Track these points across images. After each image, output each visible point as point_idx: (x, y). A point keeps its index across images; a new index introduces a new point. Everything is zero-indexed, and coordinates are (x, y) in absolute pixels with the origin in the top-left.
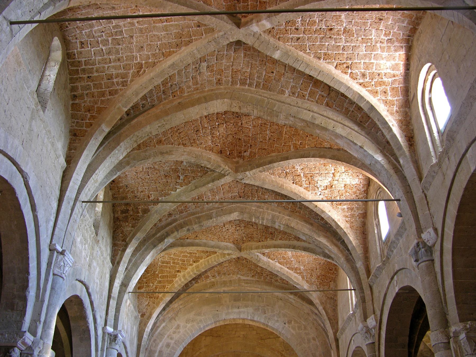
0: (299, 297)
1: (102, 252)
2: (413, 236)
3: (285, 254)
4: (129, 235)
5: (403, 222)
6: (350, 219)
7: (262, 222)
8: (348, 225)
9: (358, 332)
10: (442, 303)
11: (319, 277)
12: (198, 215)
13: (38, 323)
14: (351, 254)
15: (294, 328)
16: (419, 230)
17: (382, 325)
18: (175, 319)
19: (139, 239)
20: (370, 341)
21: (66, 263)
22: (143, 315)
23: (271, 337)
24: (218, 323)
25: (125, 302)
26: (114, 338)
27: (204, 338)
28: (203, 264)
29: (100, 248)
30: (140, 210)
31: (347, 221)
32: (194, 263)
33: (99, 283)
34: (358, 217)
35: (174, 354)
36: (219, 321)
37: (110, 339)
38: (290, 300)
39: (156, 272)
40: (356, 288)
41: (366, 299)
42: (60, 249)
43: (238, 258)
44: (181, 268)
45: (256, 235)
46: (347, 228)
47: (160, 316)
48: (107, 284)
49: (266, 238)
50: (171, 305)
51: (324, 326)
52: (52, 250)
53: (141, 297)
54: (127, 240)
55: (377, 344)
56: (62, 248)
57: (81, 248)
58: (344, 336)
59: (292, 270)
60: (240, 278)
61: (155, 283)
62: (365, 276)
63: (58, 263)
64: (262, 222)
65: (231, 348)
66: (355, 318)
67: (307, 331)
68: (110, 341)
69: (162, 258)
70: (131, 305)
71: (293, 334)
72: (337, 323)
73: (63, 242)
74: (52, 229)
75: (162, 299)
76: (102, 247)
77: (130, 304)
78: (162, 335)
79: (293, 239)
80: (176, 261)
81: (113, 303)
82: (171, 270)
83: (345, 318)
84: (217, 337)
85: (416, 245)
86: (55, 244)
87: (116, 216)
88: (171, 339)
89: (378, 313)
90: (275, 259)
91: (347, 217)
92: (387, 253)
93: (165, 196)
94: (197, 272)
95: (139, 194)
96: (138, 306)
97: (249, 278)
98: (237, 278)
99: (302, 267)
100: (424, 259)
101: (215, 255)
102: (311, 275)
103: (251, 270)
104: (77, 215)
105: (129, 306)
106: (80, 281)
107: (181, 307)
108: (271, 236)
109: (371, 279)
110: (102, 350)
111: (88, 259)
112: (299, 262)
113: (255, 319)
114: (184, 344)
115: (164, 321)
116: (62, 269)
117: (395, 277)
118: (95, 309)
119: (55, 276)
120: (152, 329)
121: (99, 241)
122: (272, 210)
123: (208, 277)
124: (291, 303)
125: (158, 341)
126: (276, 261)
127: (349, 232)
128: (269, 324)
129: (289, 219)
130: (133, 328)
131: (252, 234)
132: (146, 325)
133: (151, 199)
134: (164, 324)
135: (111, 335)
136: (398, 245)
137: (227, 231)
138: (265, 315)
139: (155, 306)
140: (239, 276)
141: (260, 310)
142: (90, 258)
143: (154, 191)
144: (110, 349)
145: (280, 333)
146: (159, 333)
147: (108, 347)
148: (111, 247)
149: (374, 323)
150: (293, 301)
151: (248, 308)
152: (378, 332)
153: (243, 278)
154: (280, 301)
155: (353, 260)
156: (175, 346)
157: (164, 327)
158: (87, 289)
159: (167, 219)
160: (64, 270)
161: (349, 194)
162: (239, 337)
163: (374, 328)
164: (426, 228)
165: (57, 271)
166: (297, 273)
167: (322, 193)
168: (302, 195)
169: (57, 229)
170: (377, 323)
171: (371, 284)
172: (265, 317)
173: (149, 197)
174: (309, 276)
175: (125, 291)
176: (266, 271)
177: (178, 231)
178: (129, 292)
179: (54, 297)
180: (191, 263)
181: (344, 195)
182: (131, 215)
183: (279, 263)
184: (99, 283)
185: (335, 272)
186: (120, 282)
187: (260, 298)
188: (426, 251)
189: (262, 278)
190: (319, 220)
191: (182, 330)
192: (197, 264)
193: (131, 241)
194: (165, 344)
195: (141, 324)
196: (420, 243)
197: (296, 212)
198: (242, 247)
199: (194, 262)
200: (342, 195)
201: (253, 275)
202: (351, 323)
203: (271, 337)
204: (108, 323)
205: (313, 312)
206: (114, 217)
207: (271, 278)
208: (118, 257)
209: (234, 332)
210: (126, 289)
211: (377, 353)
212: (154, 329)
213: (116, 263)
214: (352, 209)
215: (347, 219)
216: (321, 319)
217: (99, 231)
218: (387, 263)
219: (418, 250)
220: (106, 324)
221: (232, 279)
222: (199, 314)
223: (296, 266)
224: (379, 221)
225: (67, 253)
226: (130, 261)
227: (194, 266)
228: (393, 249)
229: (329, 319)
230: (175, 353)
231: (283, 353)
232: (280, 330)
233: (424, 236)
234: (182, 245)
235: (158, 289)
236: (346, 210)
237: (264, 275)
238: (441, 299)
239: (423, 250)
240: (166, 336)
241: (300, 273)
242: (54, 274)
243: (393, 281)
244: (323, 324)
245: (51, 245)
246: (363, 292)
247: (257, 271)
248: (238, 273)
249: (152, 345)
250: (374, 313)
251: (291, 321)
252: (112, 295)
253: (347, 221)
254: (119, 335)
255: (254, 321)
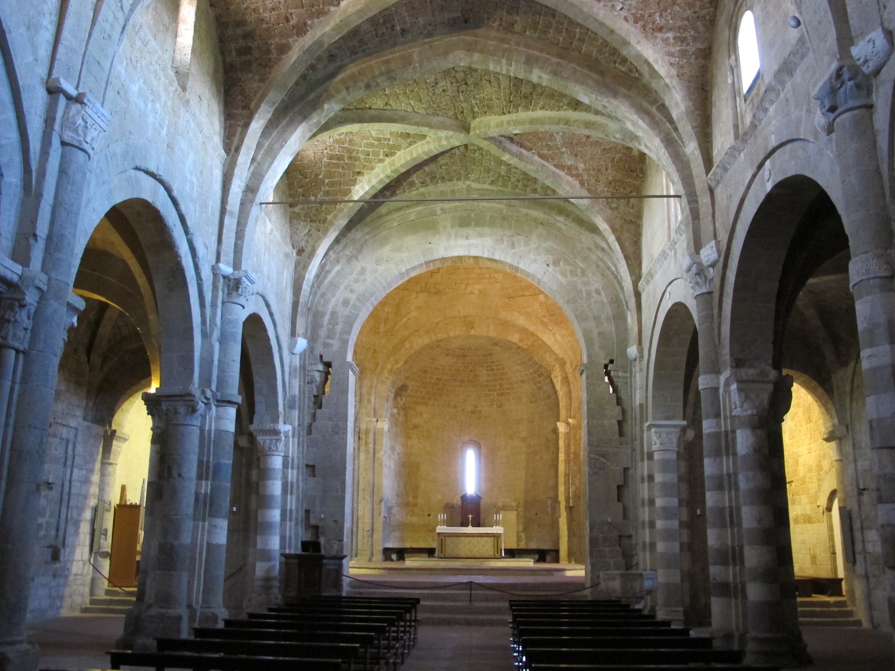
0: (574, 220)
1: (199, 125)
2: (826, 59)
3: (551, 140)
4: (255, 96)
5: (801, 41)
6: (677, 59)
7: (508, 71)
8: (674, 72)
9: (679, 276)
10: (883, 195)
11: (610, 183)
12: (385, 58)
13: (32, 241)
14: (676, 129)
15: (563, 273)
16: (845, 39)
17: (730, 260)
18: (357, 259)
19: (274, 103)
20: (704, 290)
21: (89, 121)
22: (300, 252)
23: (526, 293)
24: (431, 264)
25: (253, 221)
26: (234, 285)
27: (414, 296)
28: (403, 159)
29: (194, 116)
30: (273, 46)
31: (671, 64)
32: (386, 158)
33: (196, 183)
34: (694, 57)
35: (357, 316)
36: (434, 261)
37: (229, 286)
38: (558, 225)
39: (319, 175)
40: (682, 192)
41: (701, 213)
42: (73, 92)
43: (466, 146)
44: (364, 166)
45: (498, 101)
46: (671, 77)
47: (331, 253)
48: (217, 187)
49: (516, 107)
50: (349, 235)
51: (616, 269)
52: (54, 91)
53: (295, 221)
54: (252, 105)
55: (716, 295)
56: (77, 88)
57: (142, 106)
58: (651, 285)
59: (563, 170)
60: (469, 186)
61: (319, 196)
62: (702, 169)
63: (71, 120)
64: (508, 71)
65: (459, 312)
66: (675, 253)
67: (586, 279)
68: (228, 290)
69: (328, 148)
70: (275, 233)
71: (562, 283)
72: (640, 265)
73: (79, 78)
74: (50, 48)
75: (332, 224)
76: (197, 113)
77: (272, 230)
78: (334, 285)
79: (565, 107)
80: (354, 154)
81: (230, 223)
82: (347, 172)
83: (656, 255)
84: (435, 293)
85: (835, 74)
86: (57, 80)
87: (228, 60)
88: (352, 291)
89: (723, 237)
90: (532, 149)
91: (671, 55)
92: (754, 116)
93: (318, 18)
94: (392, 174)
95: (267, 15)
96: (291, 237)
97: (487, 186)
98: (464, 186)
99: (581, 166)
100: (851, 104)
101: (424, 141)
102: (597, 180)
103: (488, 170)
104: (112, 26)
105: (271, 234)
106: (147, 172)
107: (367, 237)
108: (524, 101)
109: (715, 174)
110: (214, 305)
111: (164, 132)
112: (576, 156)
113: (497, 257)
114: (375, 301)
115: (338, 261)
116: (80, 132)
117: (768, 163)
118: (191, 230)
119: (68, 148)
120: (317, 276)
121: (188, 102)
122: (527, 46)
123: (412, 184)
124: (559, 229)
125: (329, 295)
126: (533, 153)
127: (674, 84)
128: (521, 266)
129: (558, 63)
130: (283, 274)
131: (491, 100)
132: (305, 268)
133: (291, 23)
134: (337, 268)
135: (229, 280)
136: (782, 95)
137: (443, 94)
138: (513, 250)
139: (321, 235)
140: (468, 182)
141: (505, 242)
142: (168, 130)
143: (296, 7)
144: (229, 304)
145: (539, 282)
146: (330, 282)
147: (225, 300)
148: (223, 119)
149: (714, 256)
150: (563, 227)
151: (485, 239)
152: (721, 272)
153: (475, 185)
154: (540, 226)
155: (679, 141)
156: (357, 304)
157: (338, 272)
158: (168, 190)
159: (325, 67)
160: (85, 135)
161: (678, 9)
162: (472, 293)
163: (713, 265)
164: (863, 34)
165: (68, 136)
166: (572, 176)
167: (625, 7)
168: (585, 9)
169: (61, 49)
170: (719, 256)
171: (713, 184)
172: (515, 254)
173: (288, 20)
174: (593, 181)
175: (252, 201)
176: (516, 173)
177: (347, 88)
178: (261, 204)
179: (67, 188)
180: (381, 157)
181: (669, 11)
182: (257, 59)
183: (541, 156)
184: (196, 183)
185: (641, 175)
186: (243, 186)
187: (506, 222)
188: (858, 86)
189: (510, 187)
190: (617, 65)
191: (369, 277)
192: (393, 158)
193: (258, 106)
194: (341, 300)
195: (299, 267)
196: (845, 69)
197: (573, 50)
198: (472, 125)
199: (387, 155)
200: (666, 11)
201: (493, 181)
202: (666, 262)
203: (526, 293)
204: (222, 258)
205: (597, 246)
206: (224, 62)
207: (525, 186)
208: (236, 139)
209: (463, 286)
210: (255, 197)
211: (716, 311)
212: (322, 276)
213: (233, 149)
214: (683, 40)
215: (673, 60)
216: (611, 258)
217: (189, 83)
218: (751, 136)
219: (839, 86)
220: (218, 260)
221: (456, 188)
222: (399, 249)
223: (569, 163)
224: (737, 59)
225: (89, 98)
226: (259, 146)
227: (386, 163)
228: (767, 105)
229: (627, 258)
230: (358, 315)
231: (545, 320)
232: (539, 276)
233: (858, 51)
234: (361, 120)
235: (324, 206)
236: (672, 41)
237: (513, 180)
238: (882, 188)
239: (850, 84)
240: (342, 287)
241: (577, 176)
242: (64, 144)
243: (761, 172)
244: (615, 266)
245: (50, 80)
246: (696, 202)
247: (500, 173)
248: (467, 178)
249: (319, 302)
250: (715, 237)
251: (559, 261)
252: (228, 208)
253: (671, 64)
254: (244, 279)
255: (495, 261)
